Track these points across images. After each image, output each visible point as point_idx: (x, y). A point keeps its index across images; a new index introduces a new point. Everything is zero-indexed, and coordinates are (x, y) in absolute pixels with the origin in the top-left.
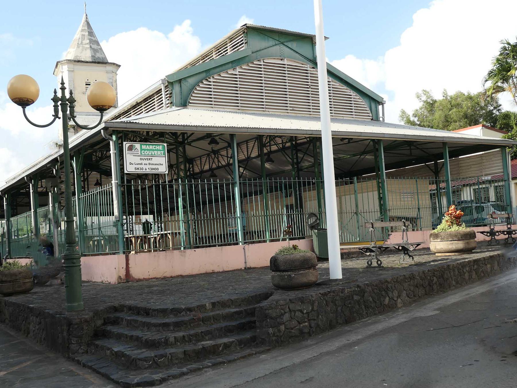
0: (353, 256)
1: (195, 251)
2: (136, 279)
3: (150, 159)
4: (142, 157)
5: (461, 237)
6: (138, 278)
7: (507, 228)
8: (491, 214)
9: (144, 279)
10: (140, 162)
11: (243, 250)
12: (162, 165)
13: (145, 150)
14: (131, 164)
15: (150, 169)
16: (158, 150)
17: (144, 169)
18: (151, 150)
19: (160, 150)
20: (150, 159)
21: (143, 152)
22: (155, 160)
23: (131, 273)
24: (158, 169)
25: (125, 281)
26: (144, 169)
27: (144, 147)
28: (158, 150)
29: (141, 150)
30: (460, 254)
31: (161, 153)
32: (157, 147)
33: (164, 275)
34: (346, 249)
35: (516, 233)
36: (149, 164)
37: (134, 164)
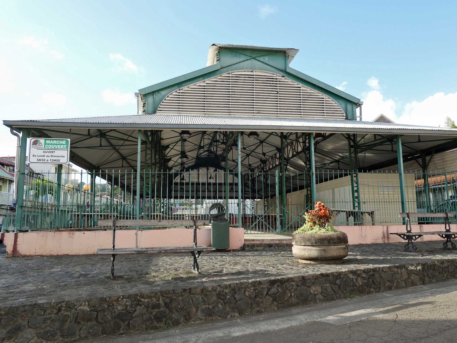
0: (258, 248)
1: (84, 233)
2: (22, 255)
3: (52, 152)
4: (45, 150)
5: (316, 243)
6: (24, 254)
7: (445, 230)
8: (407, 213)
9: (30, 255)
10: (43, 154)
11: (135, 235)
12: (64, 157)
13: (48, 144)
14: (34, 156)
15: (52, 160)
16: (61, 144)
17: (46, 160)
18: (55, 144)
19: (64, 145)
20: (52, 152)
21: (47, 146)
22: (57, 153)
23: (18, 249)
24: (59, 160)
25: (11, 256)
26: (46, 160)
27: (48, 142)
28: (61, 144)
29: (45, 144)
30: (317, 263)
31: (64, 147)
32: (60, 142)
33: (50, 253)
34: (257, 241)
35: (455, 237)
36: (52, 156)
37: (37, 156)
